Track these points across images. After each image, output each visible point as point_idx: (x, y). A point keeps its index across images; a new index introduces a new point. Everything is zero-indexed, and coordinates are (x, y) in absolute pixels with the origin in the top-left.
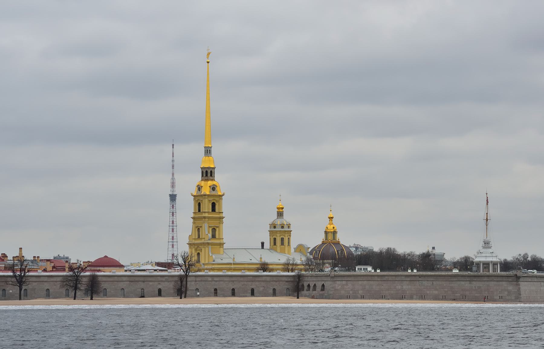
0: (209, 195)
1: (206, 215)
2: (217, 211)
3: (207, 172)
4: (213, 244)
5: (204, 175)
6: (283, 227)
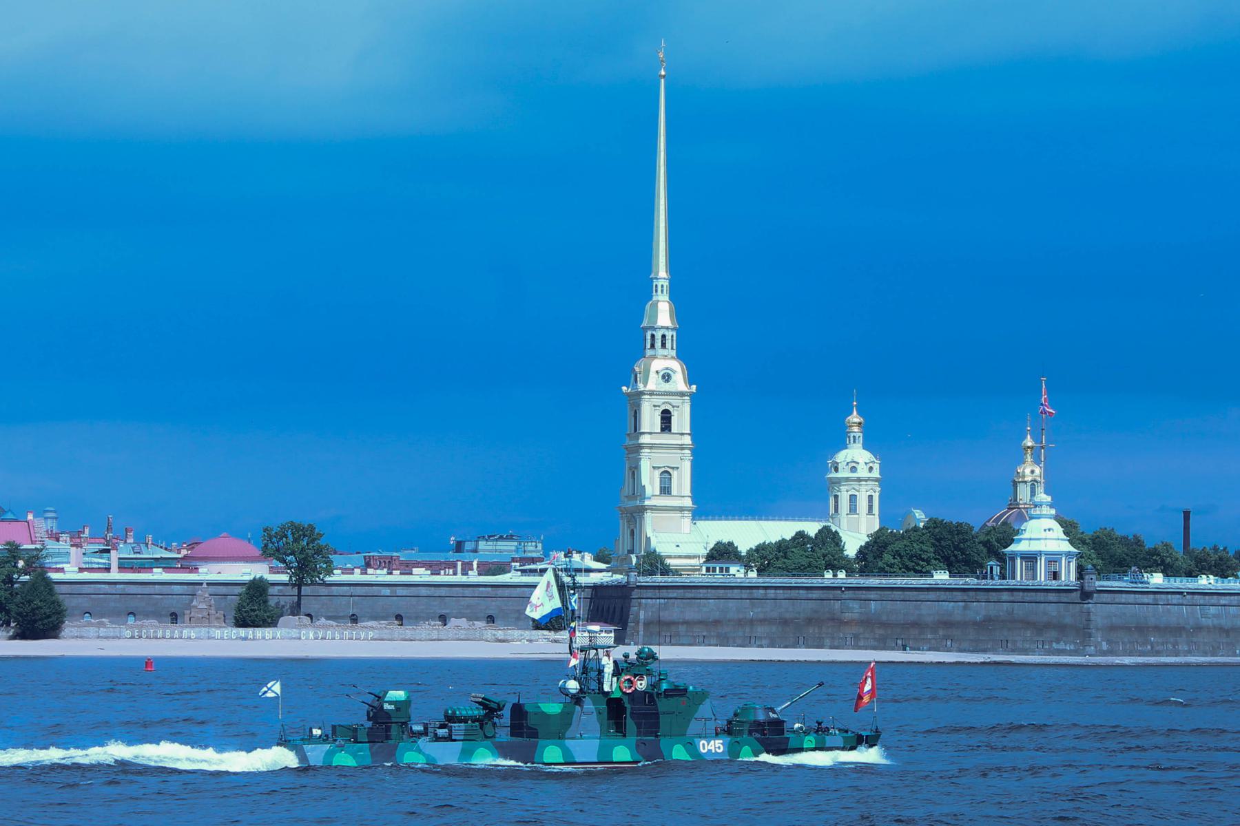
0: (652, 393)
1: (645, 439)
2: (674, 429)
3: (653, 336)
4: (655, 509)
5: (648, 346)
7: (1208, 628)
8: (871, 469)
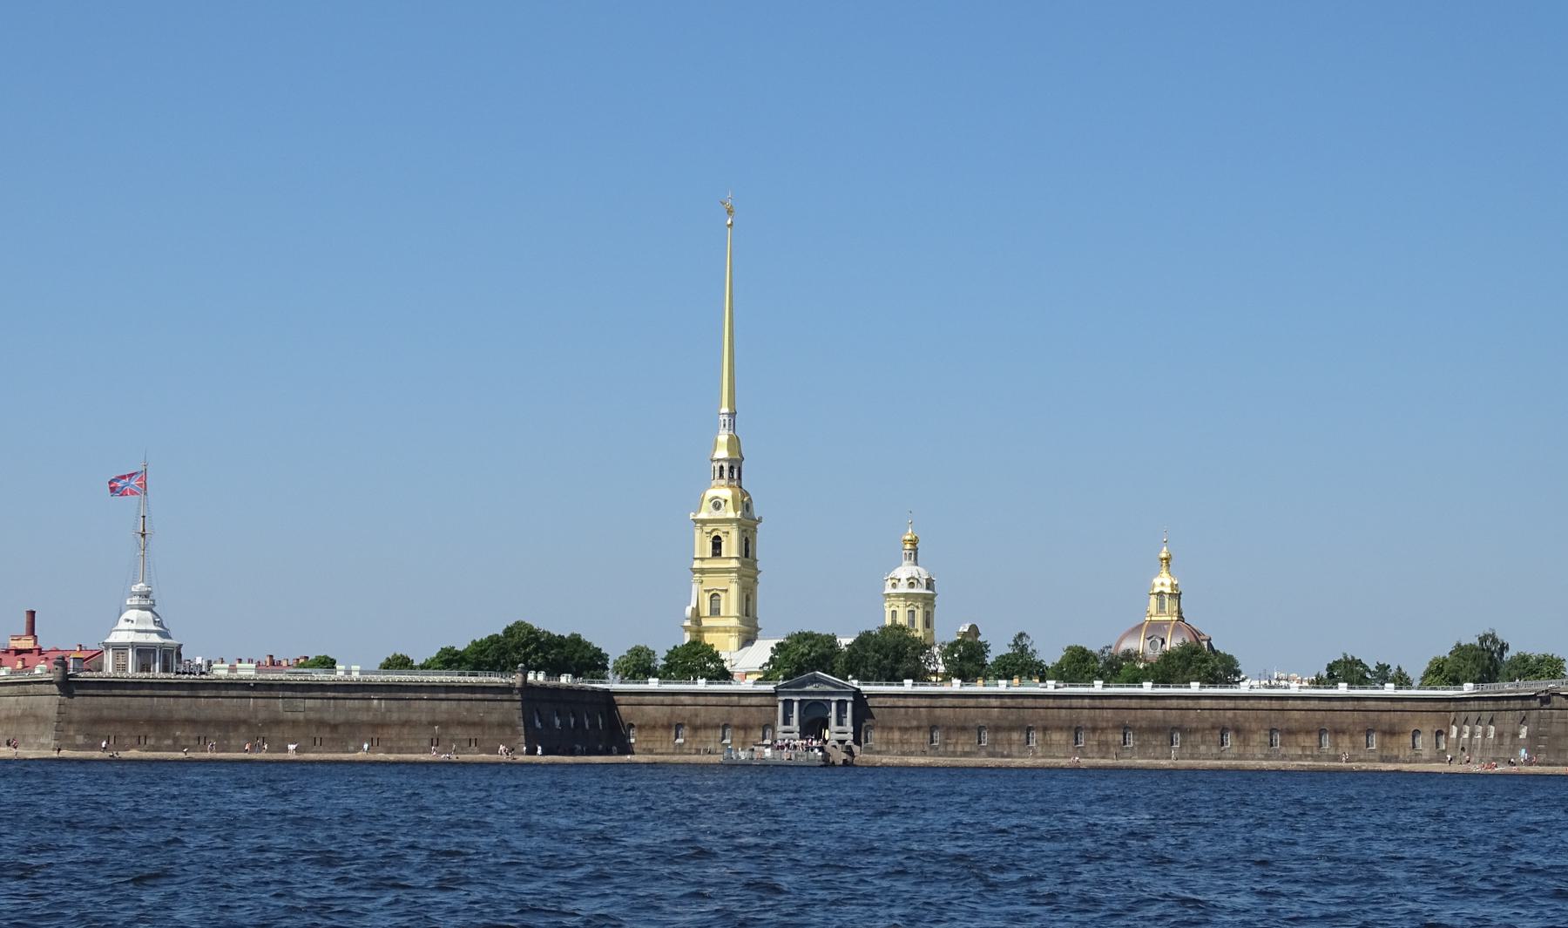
0: (704, 522)
6: (894, 586)
7: (295, 723)
8: (911, 585)
